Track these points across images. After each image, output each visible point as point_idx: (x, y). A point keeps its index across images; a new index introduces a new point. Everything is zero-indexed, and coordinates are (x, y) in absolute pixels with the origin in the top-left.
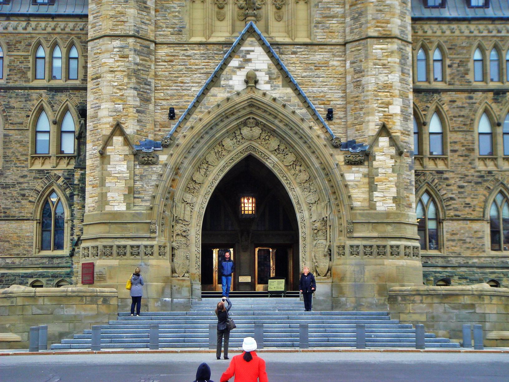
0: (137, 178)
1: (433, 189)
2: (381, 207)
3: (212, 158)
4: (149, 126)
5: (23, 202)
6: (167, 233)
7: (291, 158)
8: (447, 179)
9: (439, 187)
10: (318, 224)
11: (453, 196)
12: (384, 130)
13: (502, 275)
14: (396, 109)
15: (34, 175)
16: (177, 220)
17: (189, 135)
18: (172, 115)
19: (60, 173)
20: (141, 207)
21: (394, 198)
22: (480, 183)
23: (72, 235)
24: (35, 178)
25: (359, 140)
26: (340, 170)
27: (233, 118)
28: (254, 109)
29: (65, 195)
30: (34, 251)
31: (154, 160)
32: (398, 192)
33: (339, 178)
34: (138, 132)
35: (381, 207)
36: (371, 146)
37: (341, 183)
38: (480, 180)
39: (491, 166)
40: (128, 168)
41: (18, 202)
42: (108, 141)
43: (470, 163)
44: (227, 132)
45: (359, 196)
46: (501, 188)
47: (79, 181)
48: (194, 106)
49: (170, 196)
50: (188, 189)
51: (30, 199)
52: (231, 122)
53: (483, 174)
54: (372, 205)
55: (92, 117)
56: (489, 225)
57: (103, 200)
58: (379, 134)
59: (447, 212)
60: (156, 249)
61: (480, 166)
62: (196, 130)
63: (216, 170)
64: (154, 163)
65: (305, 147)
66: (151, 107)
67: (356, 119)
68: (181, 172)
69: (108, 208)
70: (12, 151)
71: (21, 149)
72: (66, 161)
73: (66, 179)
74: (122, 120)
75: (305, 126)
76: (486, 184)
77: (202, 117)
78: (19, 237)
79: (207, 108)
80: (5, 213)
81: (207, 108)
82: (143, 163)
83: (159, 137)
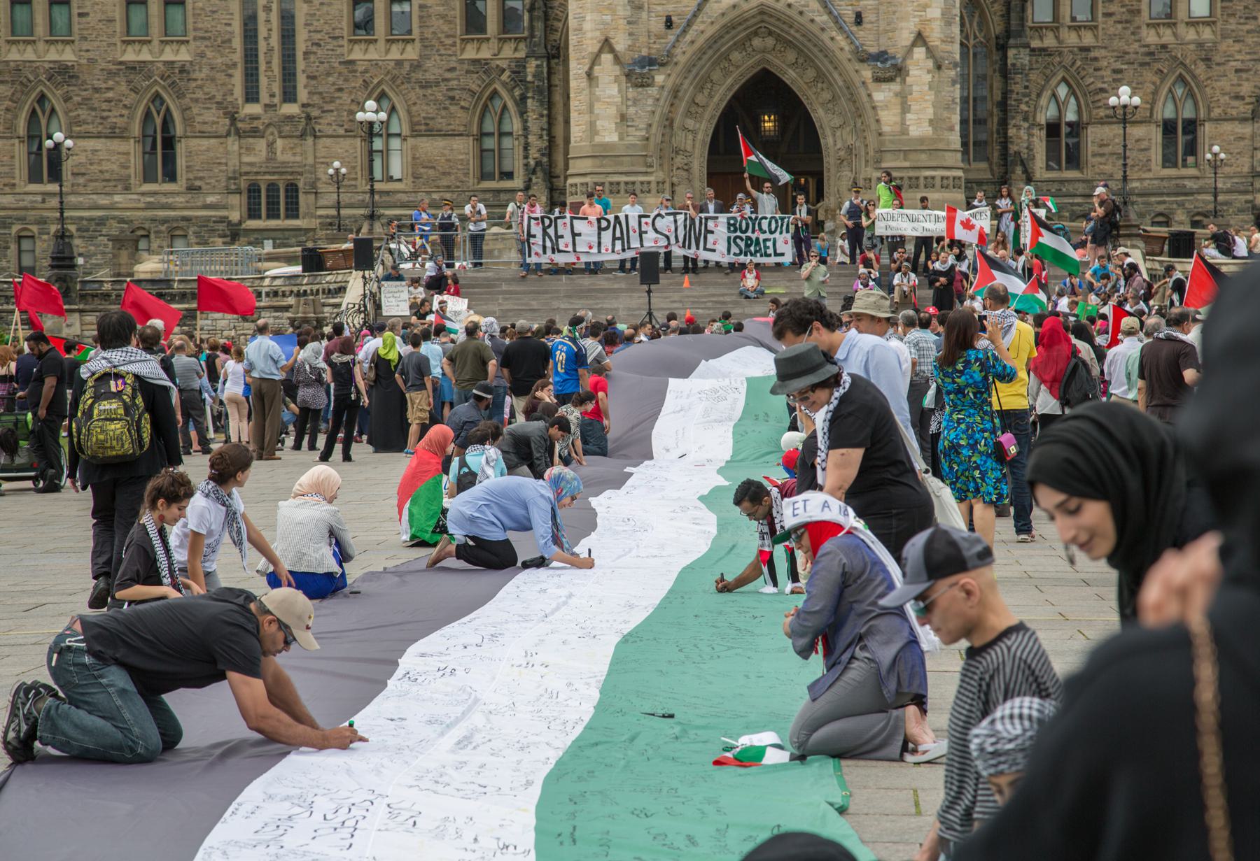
0: (630, 103)
1: (1073, 77)
2: (915, 131)
3: (716, 75)
4: (643, 39)
5: (453, 109)
6: (666, 167)
7: (811, 73)
8: (1096, 59)
9: (1083, 73)
10: (842, 153)
11: (1105, 86)
12: (920, 39)
13: (1175, 206)
14: (935, 12)
15: (466, 67)
16: (677, 152)
17: (690, 50)
18: (669, 23)
19: (504, 64)
20: (635, 136)
21: (931, 121)
22: (1148, 64)
23: (526, 157)
24: (468, 72)
25: (891, 51)
26: (867, 89)
27: (741, 28)
28: (765, 18)
29: (513, 97)
30: (471, 181)
31: (649, 81)
32: (935, 114)
33: (865, 99)
34: (630, 48)
35: (915, 131)
36: (904, 59)
37: (868, 106)
38: (1147, 59)
39: (1167, 36)
40: (620, 91)
41: (445, 108)
42: (595, 60)
43: (1133, 33)
44: (735, 44)
45: (889, 119)
46: (1180, 70)
47: (534, 76)
48: (695, 16)
49: (669, 123)
50: (688, 114)
51: (463, 103)
52: (739, 33)
53: (1152, 49)
54: (904, 131)
55: (576, 30)
56: (1160, 130)
57: (592, 130)
58: (914, 44)
59: (1094, 112)
60: (653, 186)
61: (1151, 37)
62: (697, 45)
63: (722, 90)
64: (648, 86)
65: (826, 63)
66: (644, 15)
67: (889, 24)
68: (680, 94)
69: (598, 139)
70: (431, 30)
71: (445, 28)
72: (513, 45)
73: (514, 72)
74: (611, 34)
75: (825, 37)
76: (1158, 66)
77: (704, 28)
78: (448, 160)
79: (710, 17)
80: (427, 124)
81: (710, 17)
82: (636, 86)
83: (653, 51)
